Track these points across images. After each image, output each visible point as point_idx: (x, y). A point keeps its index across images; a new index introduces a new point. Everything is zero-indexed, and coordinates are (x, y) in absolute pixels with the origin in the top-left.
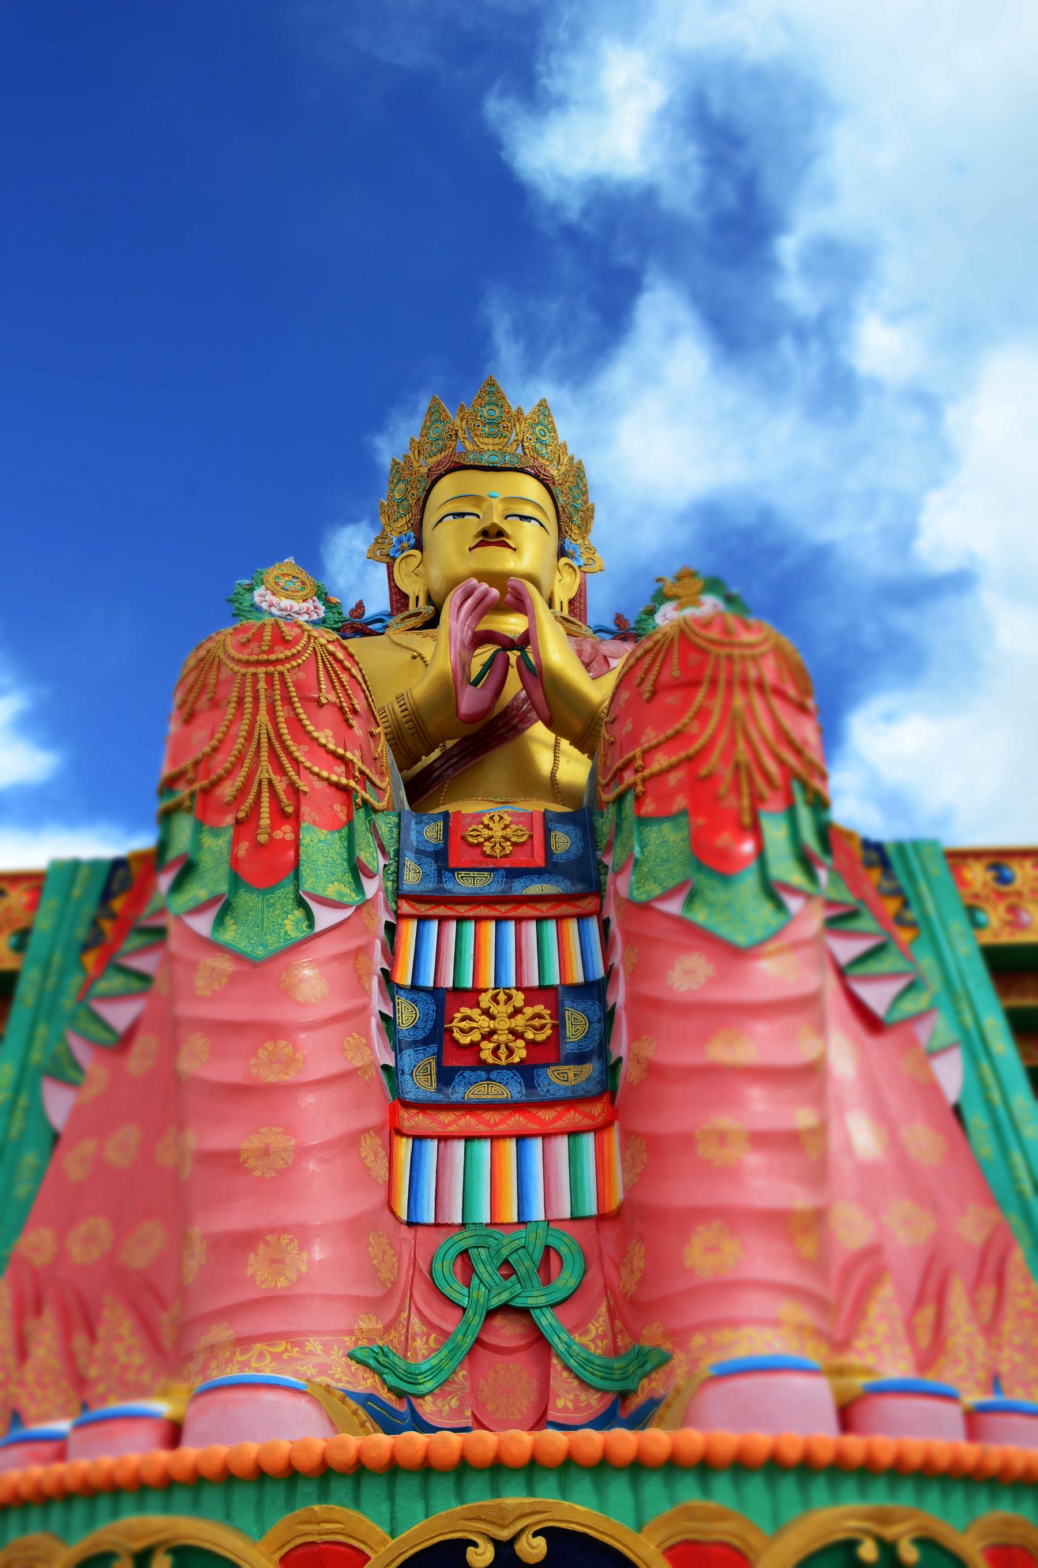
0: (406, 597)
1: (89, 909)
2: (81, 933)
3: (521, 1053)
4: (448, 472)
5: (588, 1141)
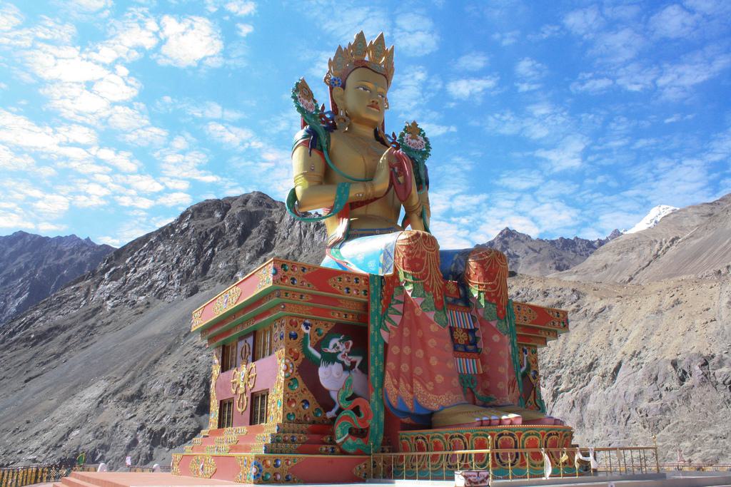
0: (336, 105)
1: (379, 289)
2: (379, 295)
3: (464, 343)
4: (363, 67)
5: (474, 360)
